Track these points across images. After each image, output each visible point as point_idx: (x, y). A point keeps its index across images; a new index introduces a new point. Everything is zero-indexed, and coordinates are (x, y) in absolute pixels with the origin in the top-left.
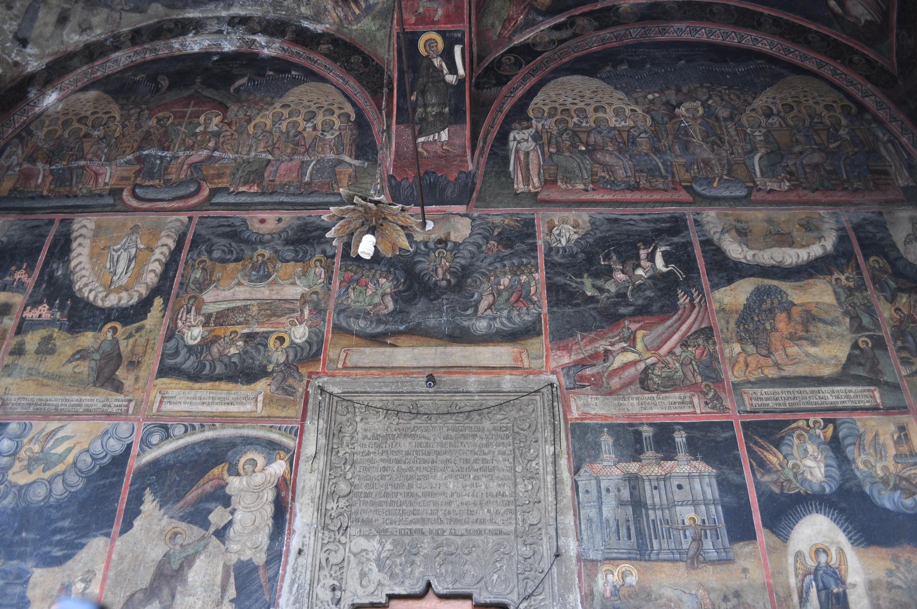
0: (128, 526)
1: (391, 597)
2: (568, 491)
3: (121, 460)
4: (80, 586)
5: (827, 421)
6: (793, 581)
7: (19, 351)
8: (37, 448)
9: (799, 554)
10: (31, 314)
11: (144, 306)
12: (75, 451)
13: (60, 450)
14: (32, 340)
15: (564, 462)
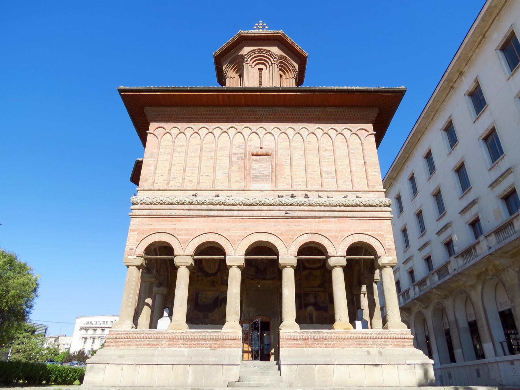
0: (220, 307)
1: (256, 316)
2: (279, 302)
3: (218, 297)
4: (215, 315)
5: (315, 293)
6: (306, 315)
7: (198, 280)
8: (205, 296)
9: (308, 312)
10: (199, 274)
11: (216, 274)
12: (211, 296)
13: (208, 296)
14: (200, 278)
15: (279, 298)
